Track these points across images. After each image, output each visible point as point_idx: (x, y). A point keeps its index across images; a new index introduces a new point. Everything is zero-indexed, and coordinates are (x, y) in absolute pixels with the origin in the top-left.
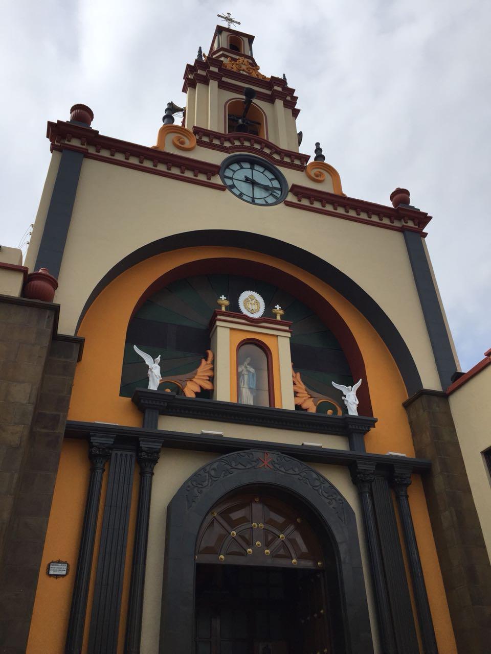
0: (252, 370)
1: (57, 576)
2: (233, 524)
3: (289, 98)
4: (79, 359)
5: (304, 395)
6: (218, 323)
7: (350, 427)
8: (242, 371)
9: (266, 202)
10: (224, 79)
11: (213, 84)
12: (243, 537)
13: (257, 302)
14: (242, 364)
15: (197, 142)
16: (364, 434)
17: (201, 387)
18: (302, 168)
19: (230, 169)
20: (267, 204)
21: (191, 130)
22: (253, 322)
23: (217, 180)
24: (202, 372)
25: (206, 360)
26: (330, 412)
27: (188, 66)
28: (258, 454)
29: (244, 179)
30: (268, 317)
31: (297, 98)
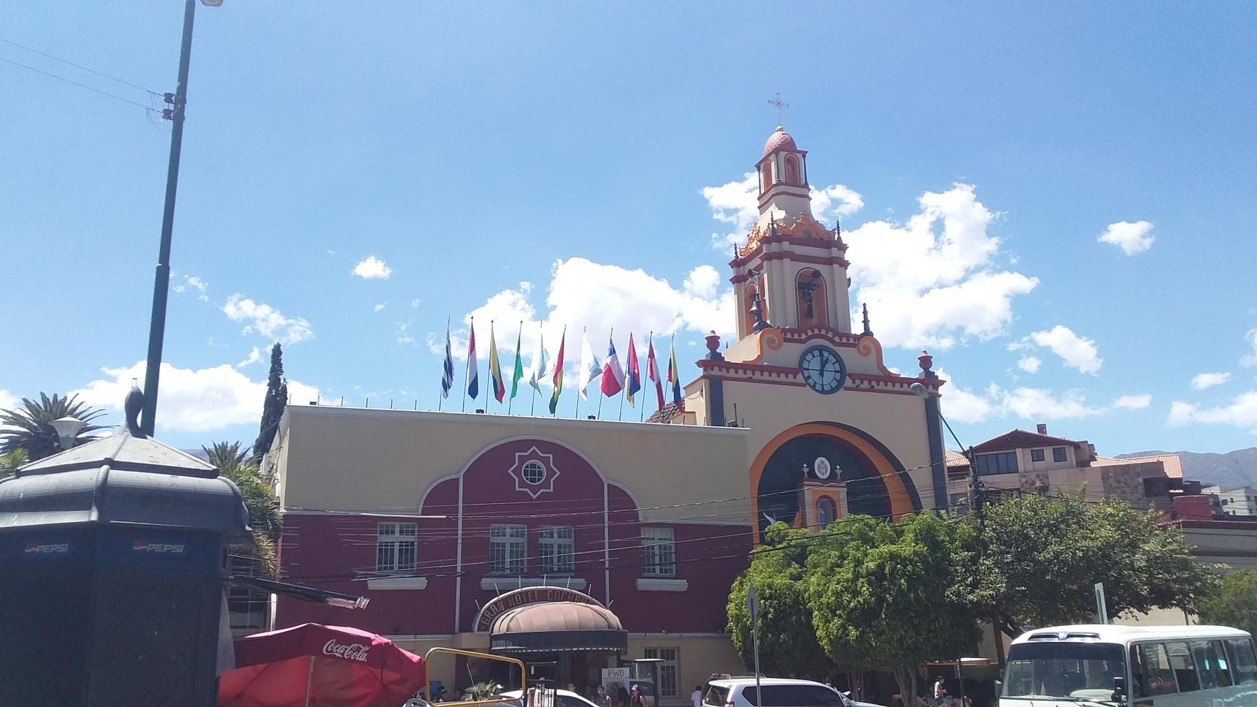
20: (833, 391)
30: (833, 476)
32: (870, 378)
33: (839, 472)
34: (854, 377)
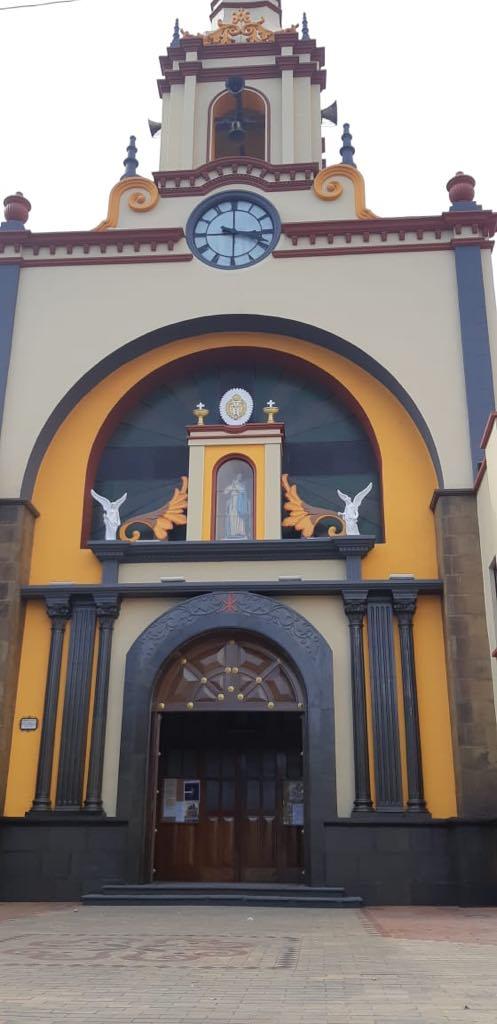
0: (240, 488)
1: (28, 730)
2: (203, 671)
3: (305, 59)
4: (35, 515)
5: (299, 513)
6: (190, 443)
7: (341, 549)
8: (231, 491)
9: (250, 257)
10: (209, 64)
11: (191, 80)
12: (213, 683)
13: (243, 403)
14: (231, 483)
15: (159, 192)
16: (364, 555)
17: (174, 524)
18: (306, 185)
19: (203, 220)
20: (253, 262)
21: (152, 179)
22: (235, 431)
23: (182, 248)
24: (175, 505)
25: (180, 489)
26: (332, 531)
27: (161, 58)
28: (222, 596)
29: (220, 231)
30: (257, 420)
31: (323, 49)
33: (271, 408)
34: (296, 231)
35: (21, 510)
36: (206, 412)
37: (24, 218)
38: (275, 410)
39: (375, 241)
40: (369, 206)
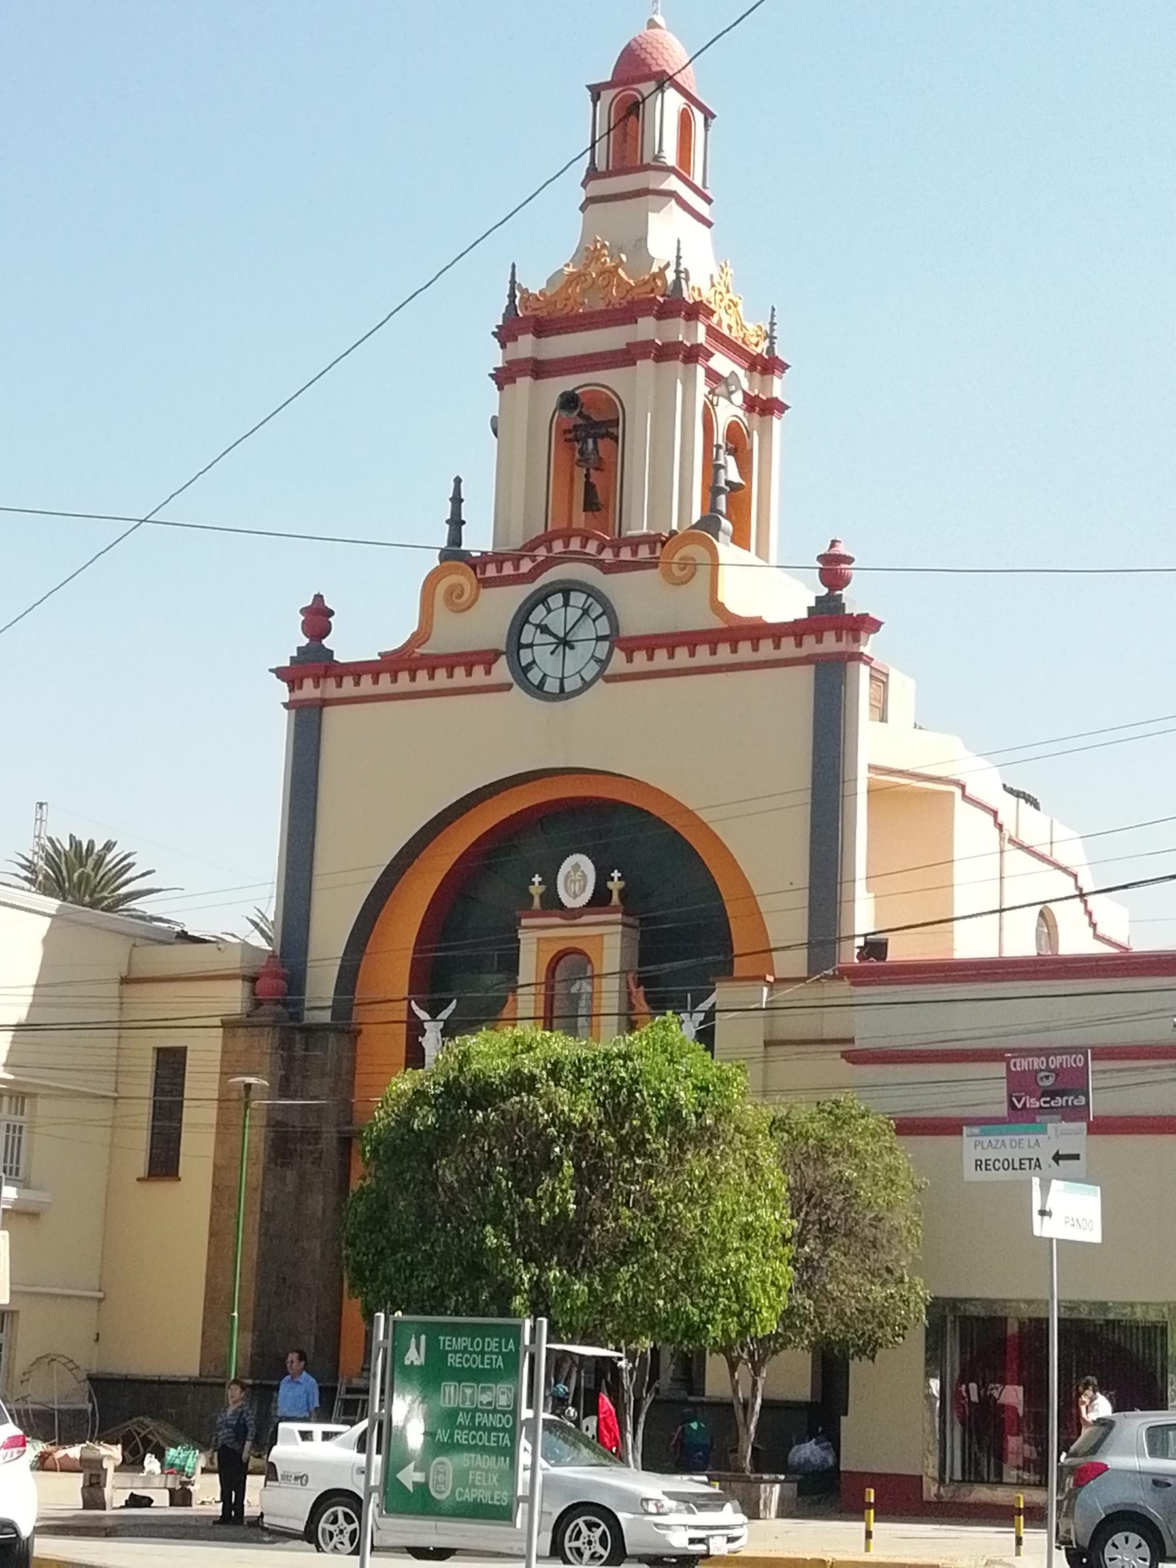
6: (522, 935)
9: (582, 679)
13: (584, 876)
20: (586, 685)
23: (502, 671)
30: (600, 899)
32: (671, 641)
34: (631, 646)
35: (332, 1038)
36: (542, 889)
37: (327, 631)
38: (622, 884)
39: (724, 653)
40: (724, 596)
